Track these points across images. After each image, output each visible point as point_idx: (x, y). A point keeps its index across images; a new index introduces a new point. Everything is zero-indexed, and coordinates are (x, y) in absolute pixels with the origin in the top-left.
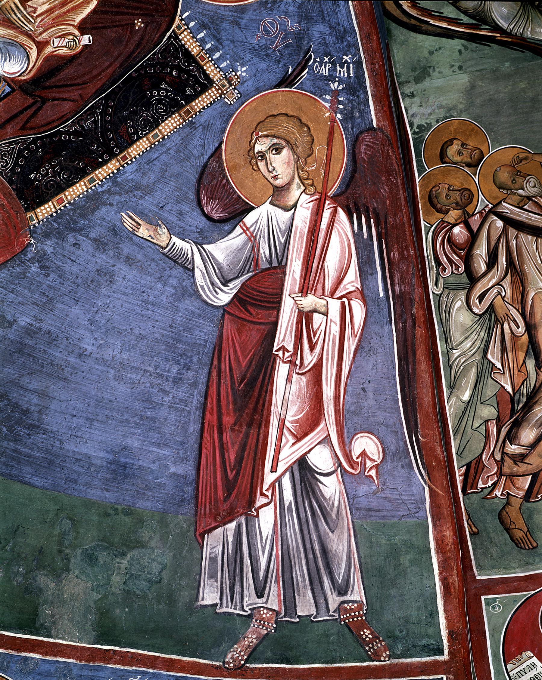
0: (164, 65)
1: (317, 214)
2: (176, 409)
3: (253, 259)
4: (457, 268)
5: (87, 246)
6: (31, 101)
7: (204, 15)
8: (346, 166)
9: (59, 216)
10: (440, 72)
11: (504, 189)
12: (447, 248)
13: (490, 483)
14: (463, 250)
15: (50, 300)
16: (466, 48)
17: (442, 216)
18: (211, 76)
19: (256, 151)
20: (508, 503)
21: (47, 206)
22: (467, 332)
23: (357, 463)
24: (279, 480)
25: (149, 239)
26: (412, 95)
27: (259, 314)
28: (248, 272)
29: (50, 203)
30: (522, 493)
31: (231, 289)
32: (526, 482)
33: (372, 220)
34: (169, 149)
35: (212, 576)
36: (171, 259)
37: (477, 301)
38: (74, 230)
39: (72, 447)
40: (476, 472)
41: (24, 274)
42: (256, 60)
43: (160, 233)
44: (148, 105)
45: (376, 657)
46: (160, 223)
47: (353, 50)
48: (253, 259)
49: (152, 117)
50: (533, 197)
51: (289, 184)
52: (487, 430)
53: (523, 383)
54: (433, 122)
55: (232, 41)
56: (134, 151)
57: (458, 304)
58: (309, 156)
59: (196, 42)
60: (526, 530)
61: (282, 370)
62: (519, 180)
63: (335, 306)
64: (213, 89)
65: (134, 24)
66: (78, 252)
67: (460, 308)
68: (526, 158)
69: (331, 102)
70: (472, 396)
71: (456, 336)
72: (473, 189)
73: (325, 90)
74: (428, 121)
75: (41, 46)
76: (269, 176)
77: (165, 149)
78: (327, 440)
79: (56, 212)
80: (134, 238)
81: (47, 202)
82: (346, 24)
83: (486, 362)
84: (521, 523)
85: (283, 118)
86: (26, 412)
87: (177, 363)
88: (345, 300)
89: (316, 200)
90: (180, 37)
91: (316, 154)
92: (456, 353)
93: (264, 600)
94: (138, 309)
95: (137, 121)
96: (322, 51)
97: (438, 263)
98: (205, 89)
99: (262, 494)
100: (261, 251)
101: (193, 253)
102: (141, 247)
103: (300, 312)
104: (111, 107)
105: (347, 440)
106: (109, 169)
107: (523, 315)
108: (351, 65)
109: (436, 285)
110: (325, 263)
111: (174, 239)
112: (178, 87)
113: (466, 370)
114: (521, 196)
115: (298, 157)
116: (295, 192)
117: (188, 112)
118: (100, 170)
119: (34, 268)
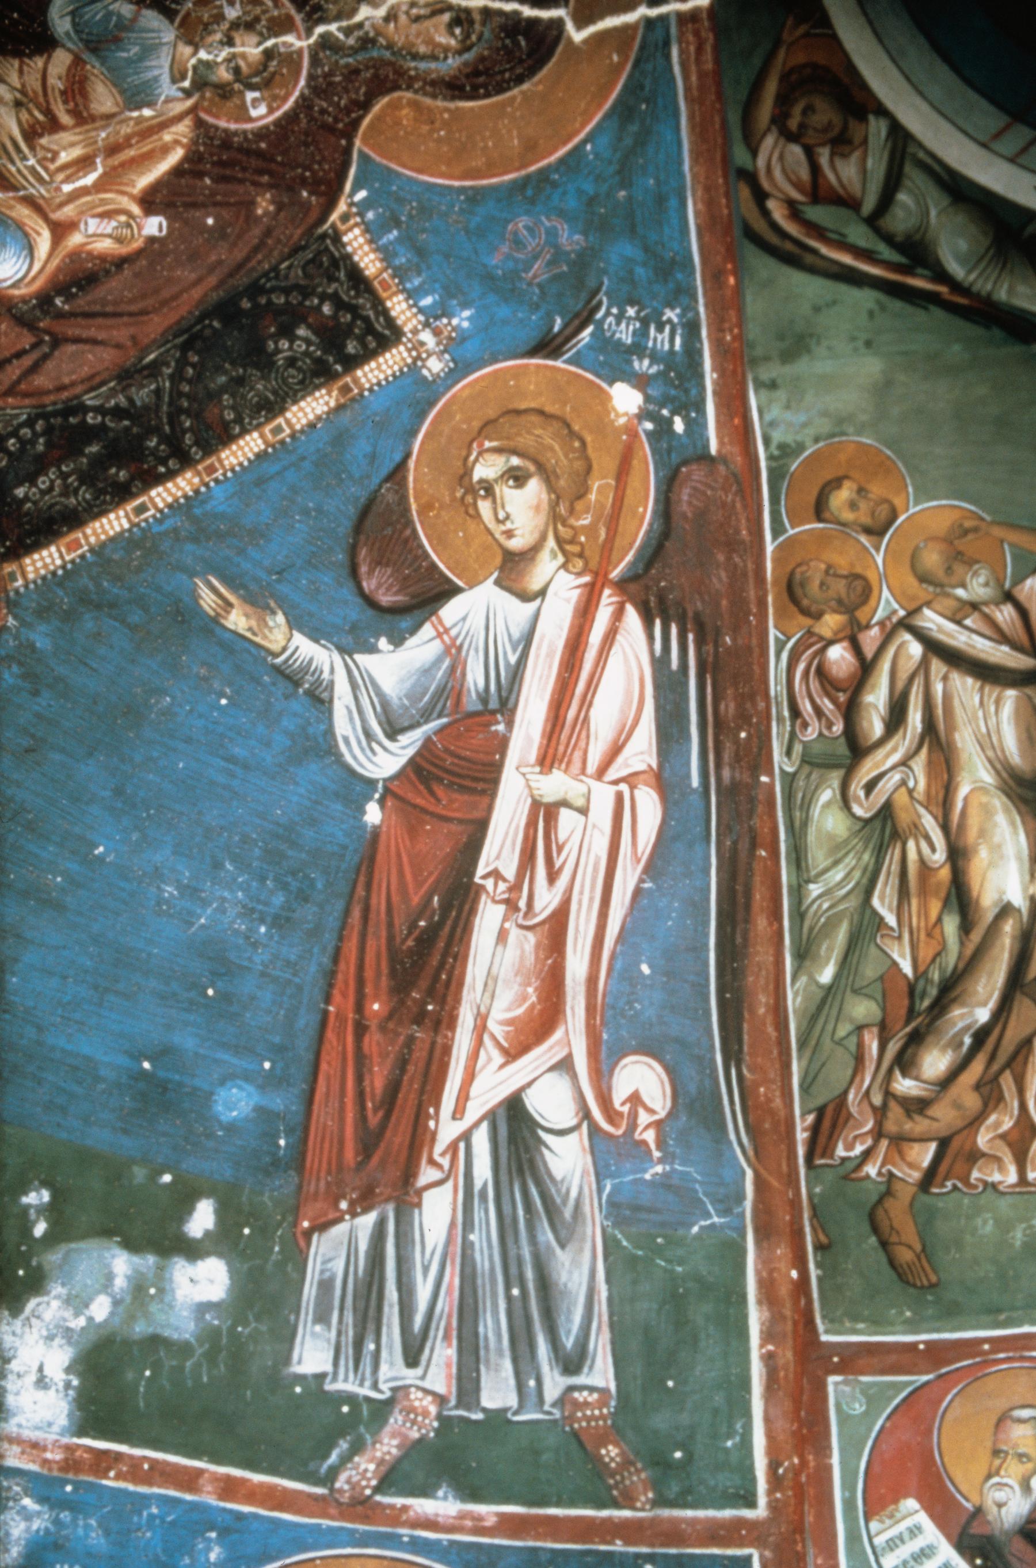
0: (306, 292)
1: (585, 612)
2: (275, 980)
3: (451, 690)
4: (830, 725)
8: (651, 525)
9: (70, 574)
10: (829, 348)
11: (930, 582)
12: (814, 684)
13: (859, 1149)
14: (844, 691)
16: (883, 308)
17: (807, 621)
18: (399, 322)
19: (476, 477)
20: (889, 1193)
21: (45, 553)
22: (837, 850)
23: (620, 1114)
24: (466, 1136)
25: (248, 635)
26: (773, 385)
27: (452, 802)
28: (440, 716)
29: (53, 549)
30: (916, 1175)
31: (403, 748)
32: (926, 1154)
33: (691, 637)
34: (303, 458)
35: (322, 1317)
37: (861, 794)
39: (62, 1042)
40: (834, 1126)
42: (492, 298)
43: (271, 623)
45: (628, 1500)
46: (272, 604)
47: (685, 300)
48: (451, 690)
49: (275, 393)
51: (535, 549)
52: (860, 1045)
53: (933, 960)
54: (808, 442)
55: (447, 256)
57: (826, 795)
59: (376, 250)
60: (918, 1247)
61: (489, 917)
62: (959, 569)
63: (603, 797)
64: (402, 348)
65: (252, 204)
67: (828, 805)
68: (975, 530)
70: (837, 977)
71: (817, 856)
72: (872, 576)
73: (624, 372)
74: (799, 438)
75: (60, 230)
76: (497, 530)
77: (293, 458)
78: (565, 1065)
79: (63, 567)
80: (218, 631)
81: (46, 545)
82: (676, 246)
83: (868, 912)
84: (909, 1233)
85: (534, 418)
87: (285, 886)
89: (585, 585)
90: (345, 239)
91: (593, 497)
92: (815, 890)
93: (419, 1371)
95: (243, 397)
97: (795, 712)
99: (432, 1162)
100: (470, 678)
101: (332, 671)
103: (536, 805)
104: (193, 366)
105: (605, 1068)
106: (179, 488)
107: (945, 827)
109: (789, 753)
110: (593, 713)
111: (299, 640)
112: (332, 338)
113: (832, 924)
114: (959, 599)
115: (558, 498)
116: (546, 566)
118: (160, 489)
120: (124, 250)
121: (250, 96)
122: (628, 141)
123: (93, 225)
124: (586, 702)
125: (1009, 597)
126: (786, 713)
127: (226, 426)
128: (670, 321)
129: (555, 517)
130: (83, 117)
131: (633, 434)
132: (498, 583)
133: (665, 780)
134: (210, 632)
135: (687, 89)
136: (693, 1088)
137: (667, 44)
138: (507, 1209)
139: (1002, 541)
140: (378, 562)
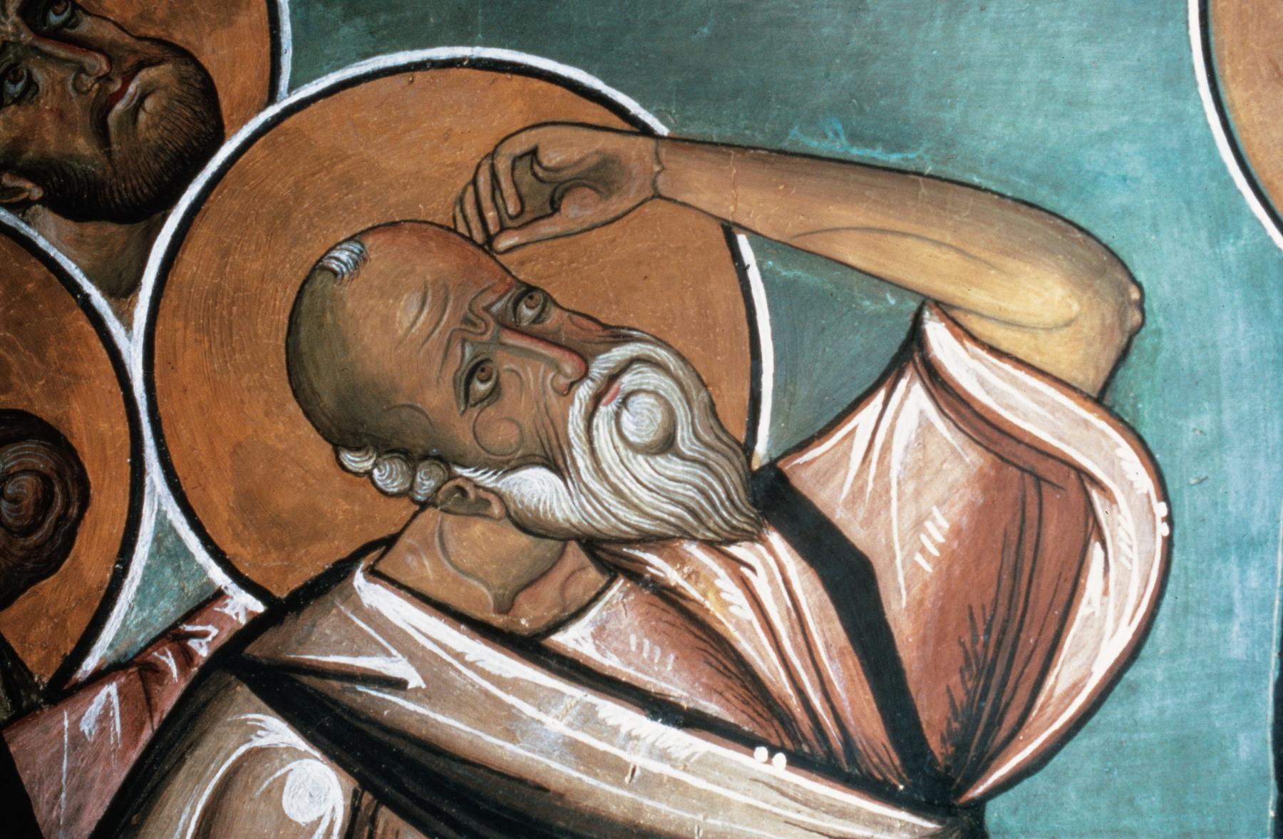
11: (385, 446)
50: (647, 540)
62: (528, 372)
68: (600, 177)
72: (93, 427)
114: (529, 525)
125: (776, 501)
139: (729, 232)
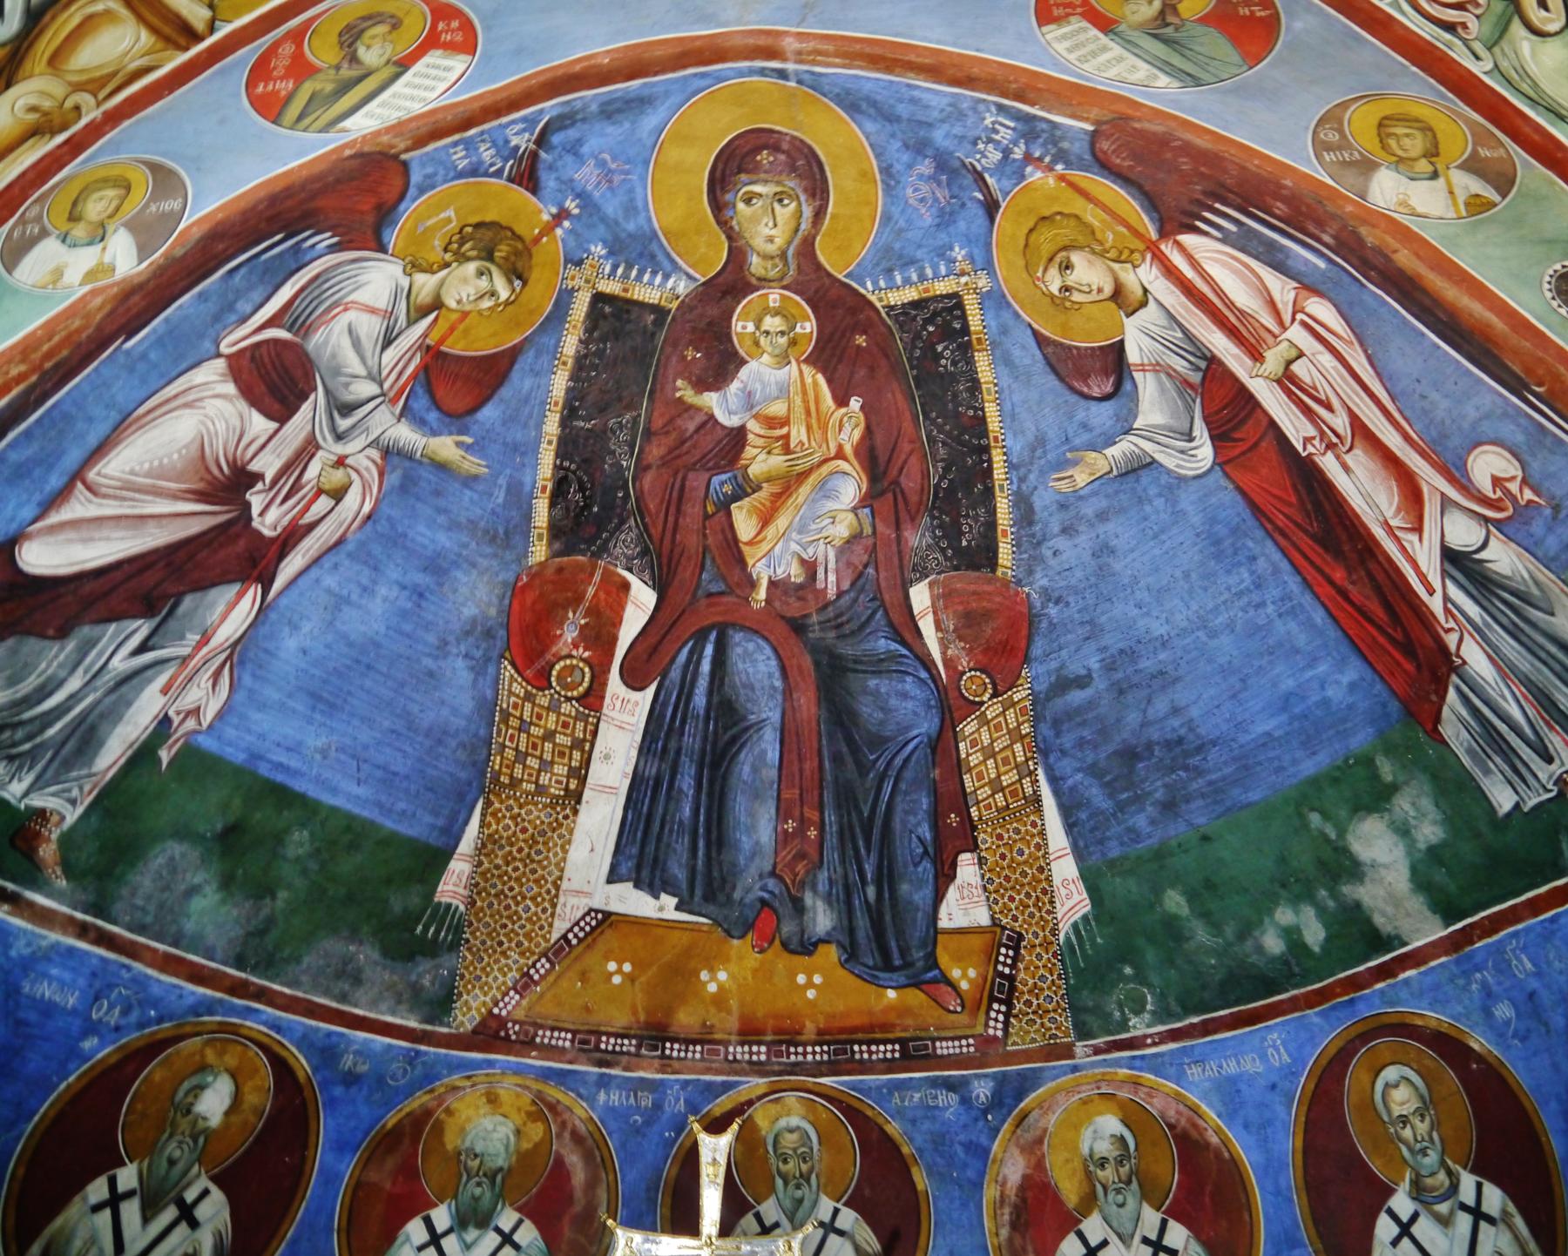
0: (918, 336)
1: (1171, 272)
2: (1287, 613)
5: (1061, 543)
6: (890, 496)
7: (877, 264)
9: (1017, 544)
15: (1091, 622)
19: (1056, 292)
23: (1500, 499)
24: (1446, 598)
27: (1248, 432)
33: (1217, 205)
36: (1127, 473)
37: (1543, 13)
38: (1039, 543)
41: (1051, 623)
44: (953, 378)
47: (981, 107)
56: (994, 424)
58: (1093, 233)
63: (1296, 334)
65: (859, 346)
66: (1064, 557)
67: (1533, 51)
69: (1038, 168)
75: (840, 455)
76: (1094, 297)
80: (1082, 493)
82: (945, 101)
85: (1033, 236)
86: (1180, 741)
87: (1239, 564)
88: (1299, 316)
94: (1157, 552)
96: (969, 147)
97: (1450, 27)
98: (960, 305)
100: (1179, 369)
102: (1095, 493)
103: (1279, 382)
105: (1464, 481)
108: (1000, 119)
109: (1478, 58)
110: (1238, 305)
111: (1110, 451)
117: (979, 340)
119: (1053, 610)
120: (863, 425)
121: (798, 329)
122: (872, 111)
123: (844, 436)
124: (1231, 305)
126: (1448, 36)
127: (975, 417)
128: (993, 123)
129: (1102, 255)
130: (785, 422)
131: (1062, 178)
132: (1128, 316)
133: (1309, 286)
134: (1081, 498)
135: (844, 66)
136: (1520, 438)
137: (813, 73)
138: (1504, 621)
140: (1085, 378)
